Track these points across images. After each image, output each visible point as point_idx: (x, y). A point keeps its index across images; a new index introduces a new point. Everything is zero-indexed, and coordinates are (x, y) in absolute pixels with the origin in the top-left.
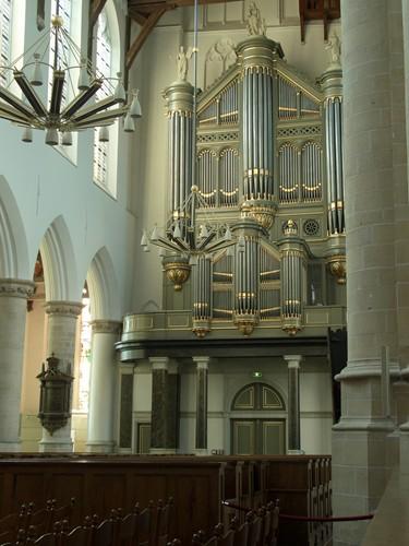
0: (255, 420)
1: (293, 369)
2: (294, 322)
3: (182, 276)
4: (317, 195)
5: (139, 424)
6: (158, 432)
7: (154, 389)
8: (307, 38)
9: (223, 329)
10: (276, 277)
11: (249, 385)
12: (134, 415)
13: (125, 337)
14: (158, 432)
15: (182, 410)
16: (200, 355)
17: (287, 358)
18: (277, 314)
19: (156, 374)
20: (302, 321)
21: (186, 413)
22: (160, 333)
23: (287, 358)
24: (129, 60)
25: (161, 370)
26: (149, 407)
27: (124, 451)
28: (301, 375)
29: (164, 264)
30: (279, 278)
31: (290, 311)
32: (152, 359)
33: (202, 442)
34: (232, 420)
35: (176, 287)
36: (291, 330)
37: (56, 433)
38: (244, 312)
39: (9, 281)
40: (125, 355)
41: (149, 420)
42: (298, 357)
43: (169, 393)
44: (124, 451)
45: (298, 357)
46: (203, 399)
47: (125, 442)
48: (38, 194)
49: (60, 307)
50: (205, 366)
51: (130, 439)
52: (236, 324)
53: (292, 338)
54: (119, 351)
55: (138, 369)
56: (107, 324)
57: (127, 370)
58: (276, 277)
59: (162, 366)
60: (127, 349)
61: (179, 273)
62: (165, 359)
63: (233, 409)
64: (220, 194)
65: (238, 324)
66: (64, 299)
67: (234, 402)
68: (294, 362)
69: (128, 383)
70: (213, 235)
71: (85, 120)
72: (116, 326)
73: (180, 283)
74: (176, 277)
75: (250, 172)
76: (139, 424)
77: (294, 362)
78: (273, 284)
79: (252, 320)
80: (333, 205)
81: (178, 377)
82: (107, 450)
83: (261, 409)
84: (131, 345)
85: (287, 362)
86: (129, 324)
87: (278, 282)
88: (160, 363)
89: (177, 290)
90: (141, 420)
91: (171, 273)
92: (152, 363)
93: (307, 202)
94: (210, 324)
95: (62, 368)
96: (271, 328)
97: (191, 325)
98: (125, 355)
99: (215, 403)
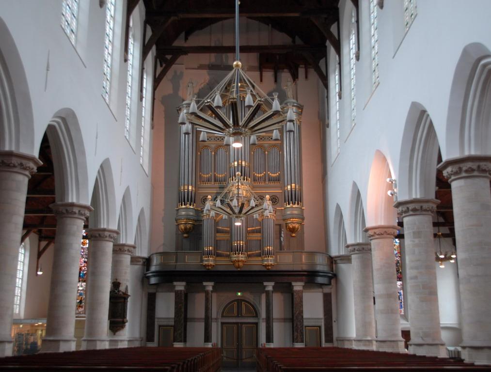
0: (237, 323)
1: (268, 291)
2: (270, 261)
3: (190, 228)
4: (277, 179)
5: (160, 326)
6: (180, 331)
7: (176, 303)
8: (263, 80)
9: (222, 264)
10: (258, 231)
11: (233, 301)
12: (156, 320)
13: (153, 269)
14: (180, 331)
15: (189, 316)
18: (259, 255)
19: (178, 294)
20: (276, 260)
21: (194, 319)
22: (181, 267)
23: (265, 284)
24: (156, 85)
25: (181, 291)
26: (172, 315)
27: (150, 345)
28: (273, 294)
29: (176, 220)
30: (260, 232)
31: (269, 254)
32: (175, 283)
33: (207, 339)
34: (222, 323)
35: (185, 235)
36: (268, 266)
37: (117, 333)
38: (239, 254)
39: (104, 230)
40: (153, 280)
41: (173, 323)
42: (273, 284)
43: (182, 304)
44: (150, 345)
45: (273, 284)
46: (208, 309)
47: (150, 337)
48: (121, 172)
50: (210, 288)
51: (153, 336)
52: (232, 262)
53: (269, 271)
54: (148, 278)
58: (258, 231)
59: (182, 288)
60: (154, 276)
61: (188, 226)
62: (184, 283)
63: (223, 316)
64: (215, 175)
65: (234, 262)
66: (124, 242)
67: (223, 312)
68: (269, 286)
70: (243, 205)
71: (256, 128)
72: (144, 260)
73: (187, 233)
74: (186, 229)
76: (160, 326)
77: (269, 286)
78: (257, 236)
79: (243, 259)
80: (289, 187)
81: (186, 295)
82: (137, 344)
83: (242, 316)
84: (158, 274)
85: (265, 287)
86: (155, 261)
87: (259, 235)
88: (180, 286)
89: (186, 237)
90: (161, 324)
91: (182, 227)
92: (174, 286)
93: (272, 184)
94: (215, 261)
95: (122, 288)
96: (256, 264)
97: (202, 261)
98: (153, 280)
99: (214, 314)
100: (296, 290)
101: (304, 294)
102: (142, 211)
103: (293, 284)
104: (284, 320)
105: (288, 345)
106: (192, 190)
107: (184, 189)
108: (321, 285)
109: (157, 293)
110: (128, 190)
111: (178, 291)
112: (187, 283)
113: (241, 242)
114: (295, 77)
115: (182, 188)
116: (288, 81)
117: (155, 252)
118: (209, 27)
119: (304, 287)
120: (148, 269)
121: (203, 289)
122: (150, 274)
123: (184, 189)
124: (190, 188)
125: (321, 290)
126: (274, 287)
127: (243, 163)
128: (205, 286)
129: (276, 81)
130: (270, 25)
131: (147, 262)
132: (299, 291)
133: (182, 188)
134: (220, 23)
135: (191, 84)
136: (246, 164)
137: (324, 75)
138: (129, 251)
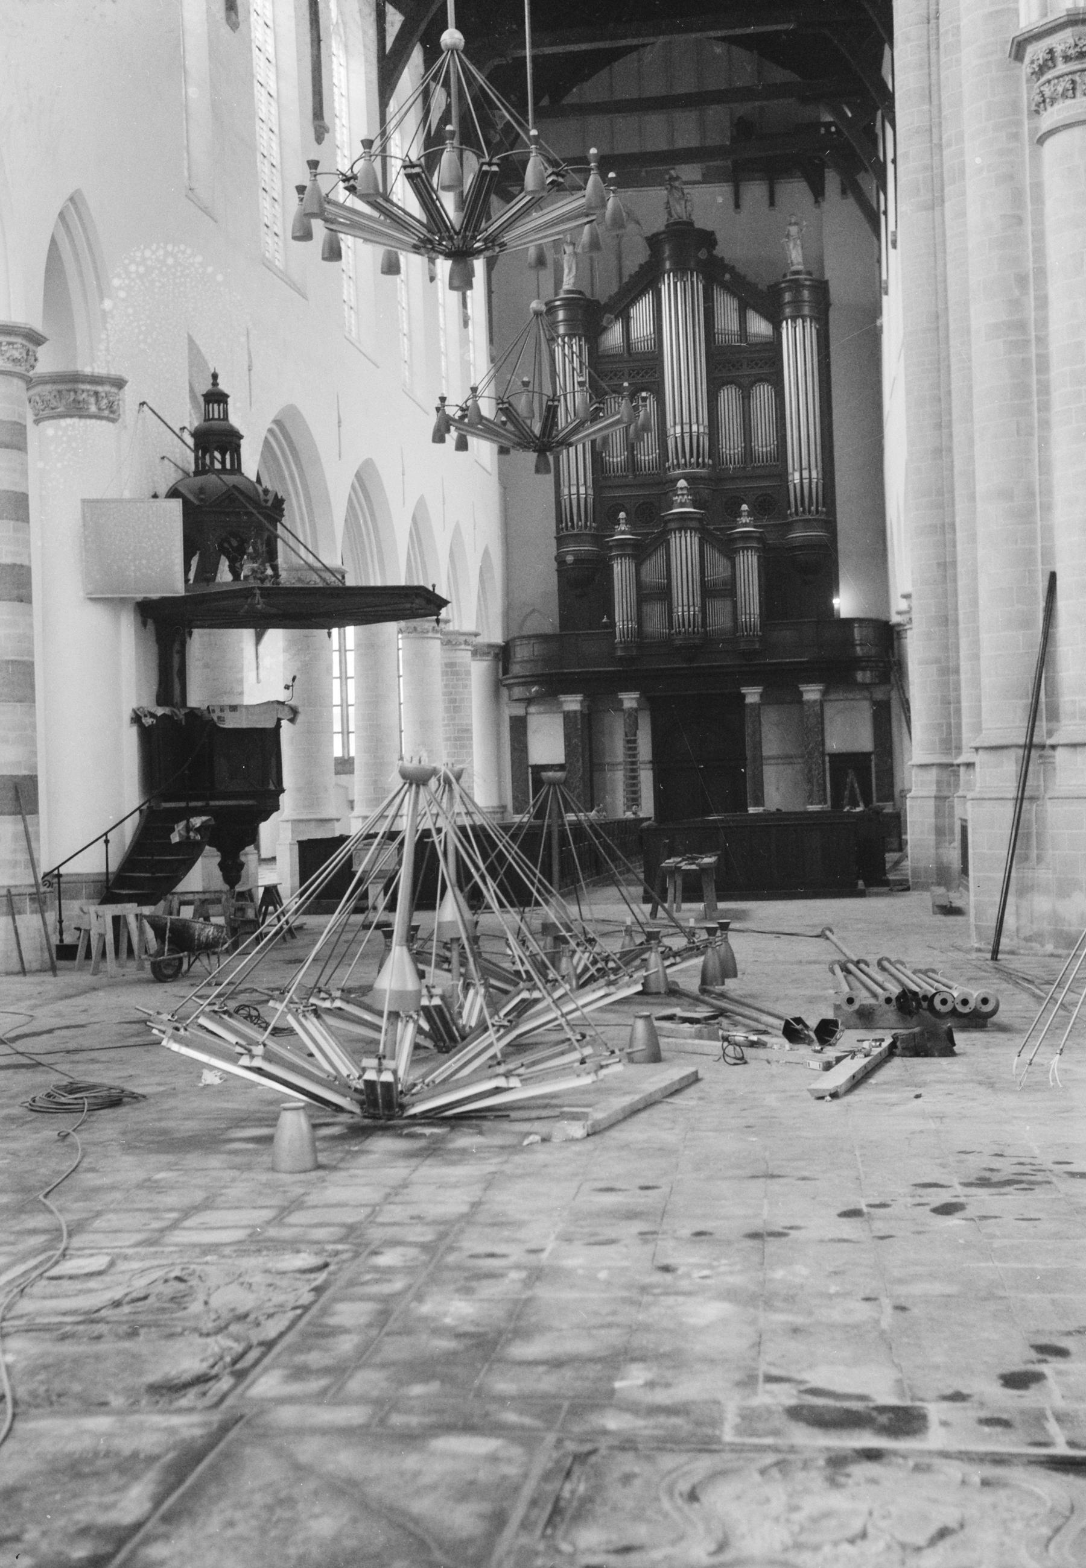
13: (516, 669)
16: (627, 690)
17: (744, 690)
19: (568, 717)
23: (744, 690)
25: (575, 712)
32: (562, 698)
33: (634, 799)
42: (759, 690)
45: (759, 690)
49: (452, 638)
50: (634, 705)
55: (532, 709)
56: (486, 650)
57: (519, 710)
69: (519, 728)
72: (497, 651)
75: (678, 429)
80: (797, 475)
86: (522, 652)
88: (573, 703)
92: (561, 704)
100: (808, 701)
101: (829, 711)
102: (486, 552)
103: (803, 688)
104: (786, 759)
105: (799, 808)
106: (586, 494)
107: (570, 494)
108: (865, 686)
109: (529, 717)
110: (457, 531)
111: (569, 712)
112: (586, 696)
113: (692, 609)
114: (818, 193)
115: (566, 492)
116: (790, 224)
117: (516, 635)
118: (606, 70)
119: (825, 693)
120: (506, 671)
121: (618, 706)
122: (512, 681)
123: (570, 494)
124: (582, 490)
125: (866, 694)
126: (761, 695)
127: (695, 428)
128: (621, 701)
129: (772, 203)
130: (755, 52)
131: (503, 655)
132: (815, 701)
133: (566, 492)
134: (635, 55)
135: (571, 247)
136: (701, 430)
137: (871, 206)
138: (466, 643)
